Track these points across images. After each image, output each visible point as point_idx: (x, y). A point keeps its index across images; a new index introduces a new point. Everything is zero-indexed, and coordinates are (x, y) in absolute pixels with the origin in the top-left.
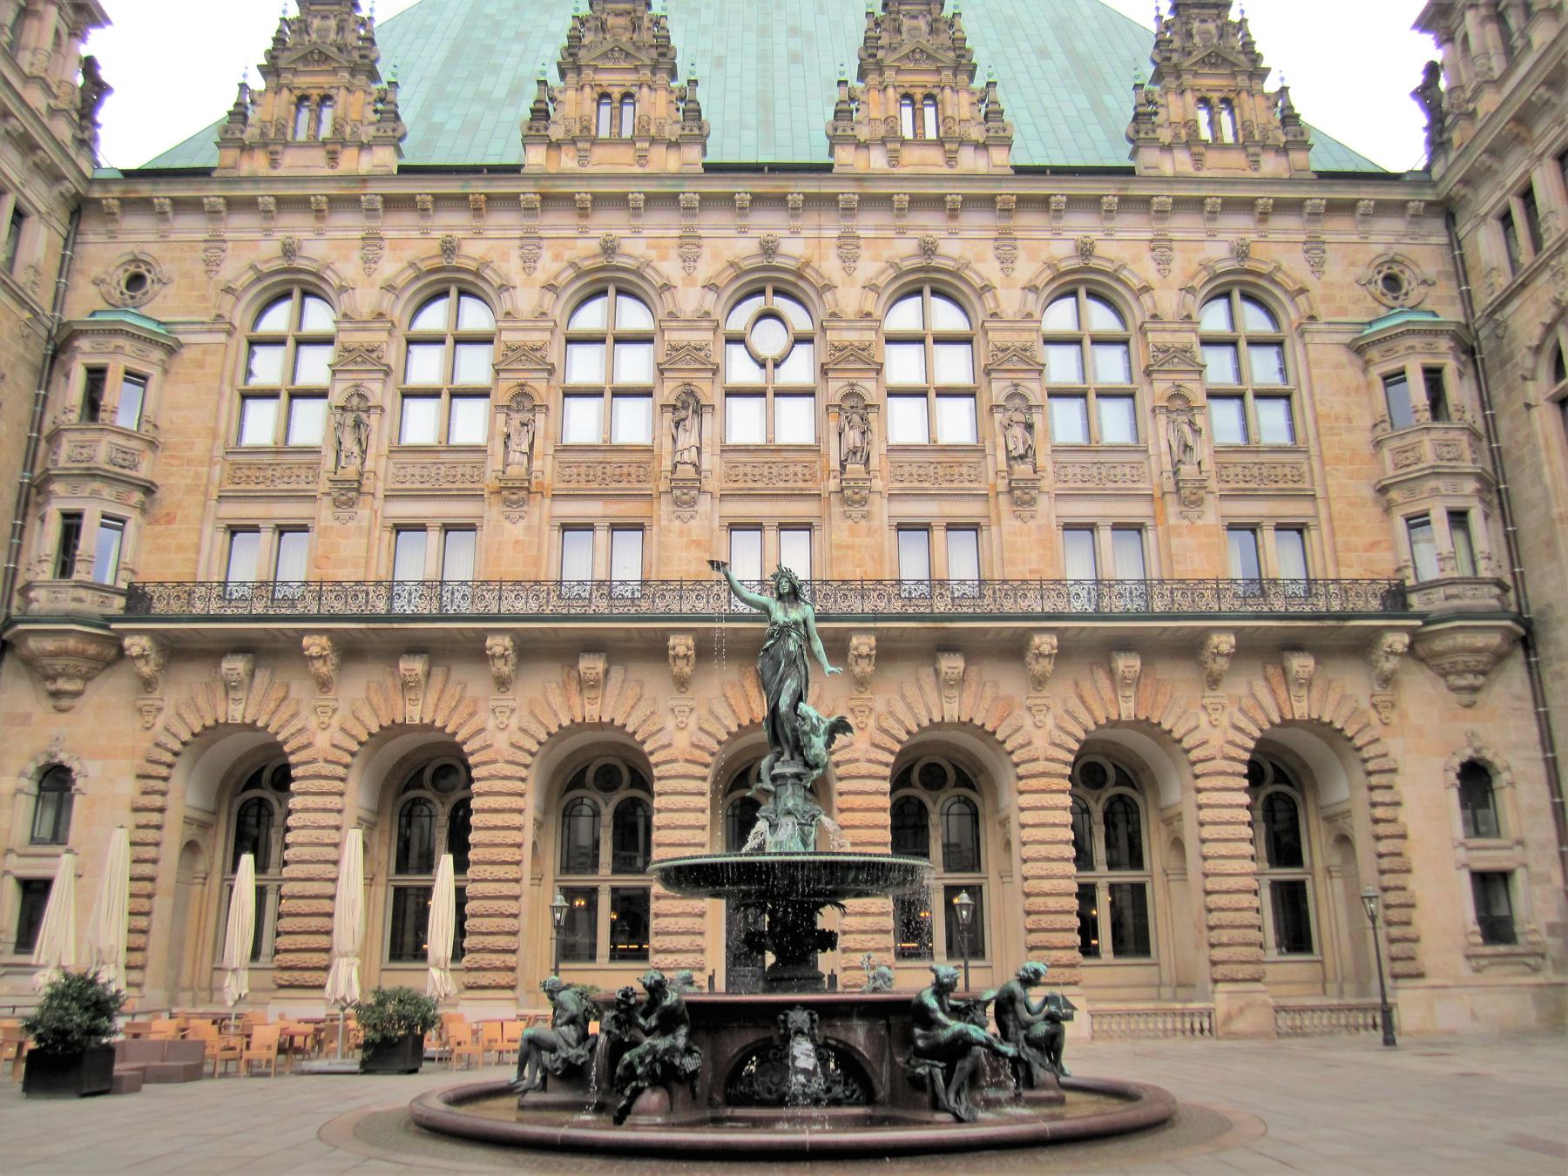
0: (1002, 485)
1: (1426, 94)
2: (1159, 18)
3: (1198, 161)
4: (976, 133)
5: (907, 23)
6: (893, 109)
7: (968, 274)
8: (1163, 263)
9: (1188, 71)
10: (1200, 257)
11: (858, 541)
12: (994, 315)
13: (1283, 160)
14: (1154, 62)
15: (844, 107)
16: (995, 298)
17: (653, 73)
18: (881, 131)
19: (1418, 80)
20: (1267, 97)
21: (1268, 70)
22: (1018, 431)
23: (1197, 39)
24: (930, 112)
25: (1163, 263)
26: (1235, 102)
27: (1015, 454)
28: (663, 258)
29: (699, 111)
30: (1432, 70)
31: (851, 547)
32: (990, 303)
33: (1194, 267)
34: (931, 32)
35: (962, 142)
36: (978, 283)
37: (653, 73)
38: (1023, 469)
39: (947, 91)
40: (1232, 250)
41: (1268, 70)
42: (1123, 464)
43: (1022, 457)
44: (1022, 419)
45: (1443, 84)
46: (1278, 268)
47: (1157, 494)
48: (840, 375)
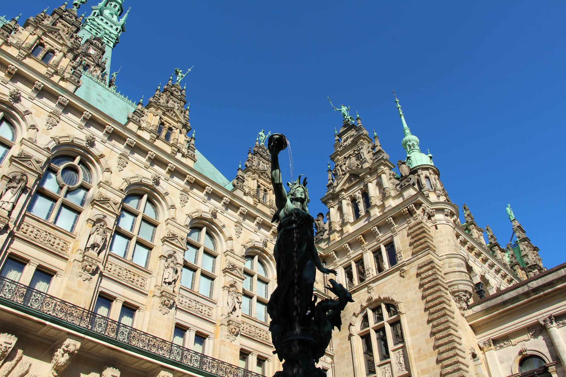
0: (158, 293)
4: (184, 150)
5: (171, 102)
8: (239, 233)
11: (81, 290)
15: (139, 112)
16: (175, 213)
17: (68, 52)
22: (171, 270)
25: (239, 233)
27: (167, 281)
28: (38, 116)
29: (81, 76)
31: (76, 292)
33: (248, 240)
37: (68, 52)
38: (169, 289)
42: (206, 306)
43: (170, 283)
44: (173, 266)
47: (218, 324)
48: (100, 209)
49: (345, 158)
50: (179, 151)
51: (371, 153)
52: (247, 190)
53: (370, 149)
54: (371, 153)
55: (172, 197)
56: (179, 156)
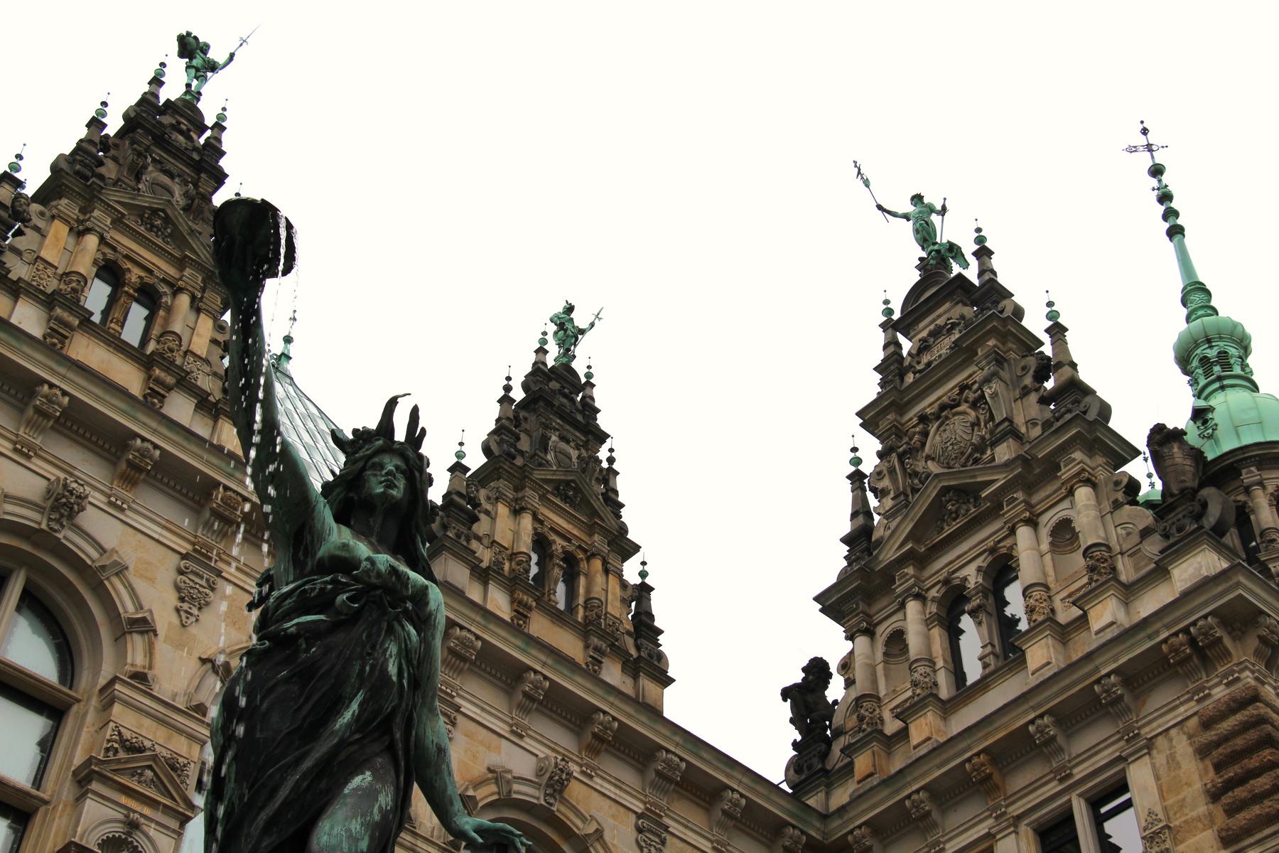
1: (806, 697)
2: (505, 400)
3: (521, 612)
4: (206, 382)
5: (152, 174)
6: (85, 265)
7: (117, 587)
9: (537, 486)
10: (494, 759)
12: (140, 677)
13: (629, 681)
14: (486, 449)
16: (150, 651)
18: (51, 285)
19: (798, 677)
20: (624, 585)
21: (636, 548)
23: (550, 457)
24: (138, 314)
26: (584, 565)
30: (817, 671)
32: (136, 655)
34: (187, 209)
35: (184, 383)
36: (128, 608)
39: (184, 300)
40: (540, 772)
41: (636, 548)
45: (835, 690)
46: (599, 834)
49: (923, 419)
50: (184, 383)
51: (1033, 398)
52: (486, 556)
53: (1028, 381)
54: (1033, 398)
55: (140, 586)
56: (180, 408)
